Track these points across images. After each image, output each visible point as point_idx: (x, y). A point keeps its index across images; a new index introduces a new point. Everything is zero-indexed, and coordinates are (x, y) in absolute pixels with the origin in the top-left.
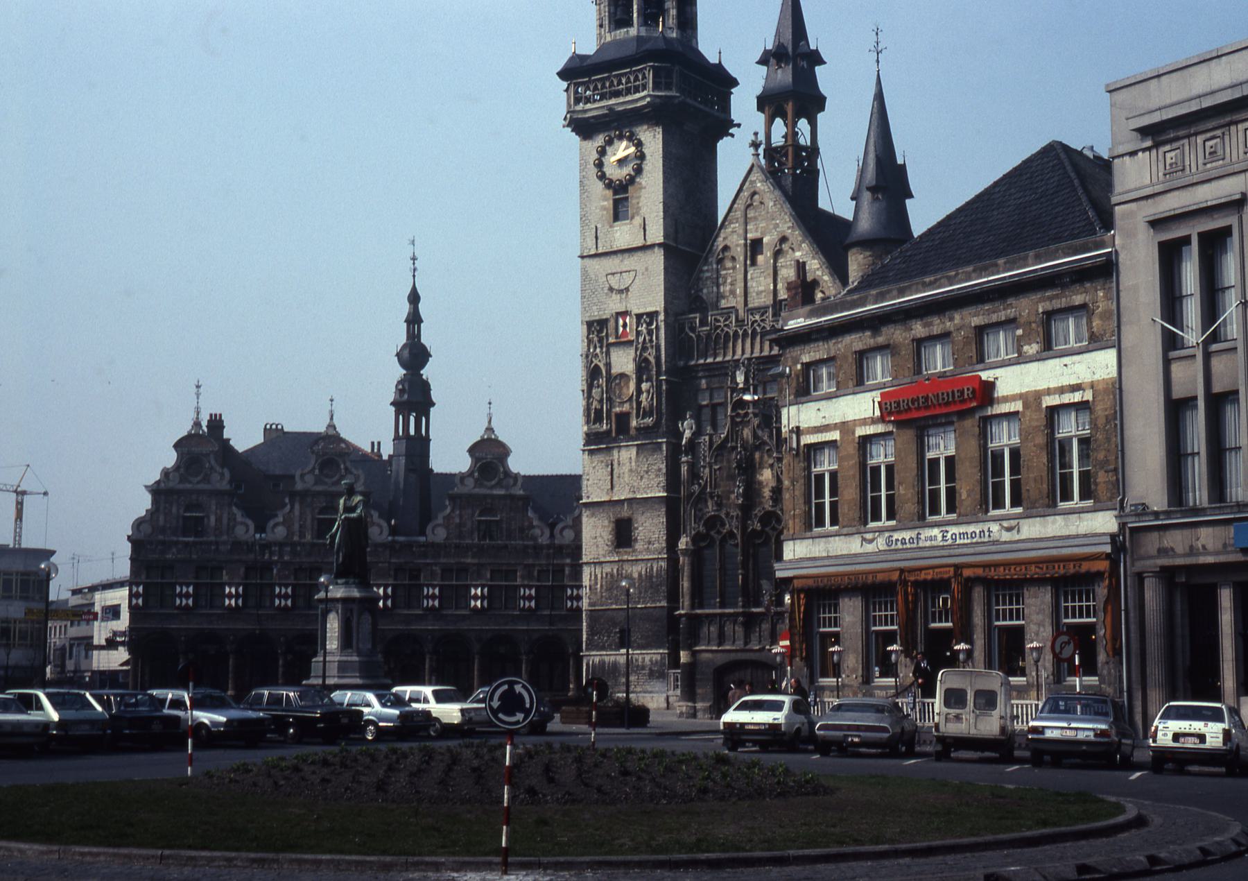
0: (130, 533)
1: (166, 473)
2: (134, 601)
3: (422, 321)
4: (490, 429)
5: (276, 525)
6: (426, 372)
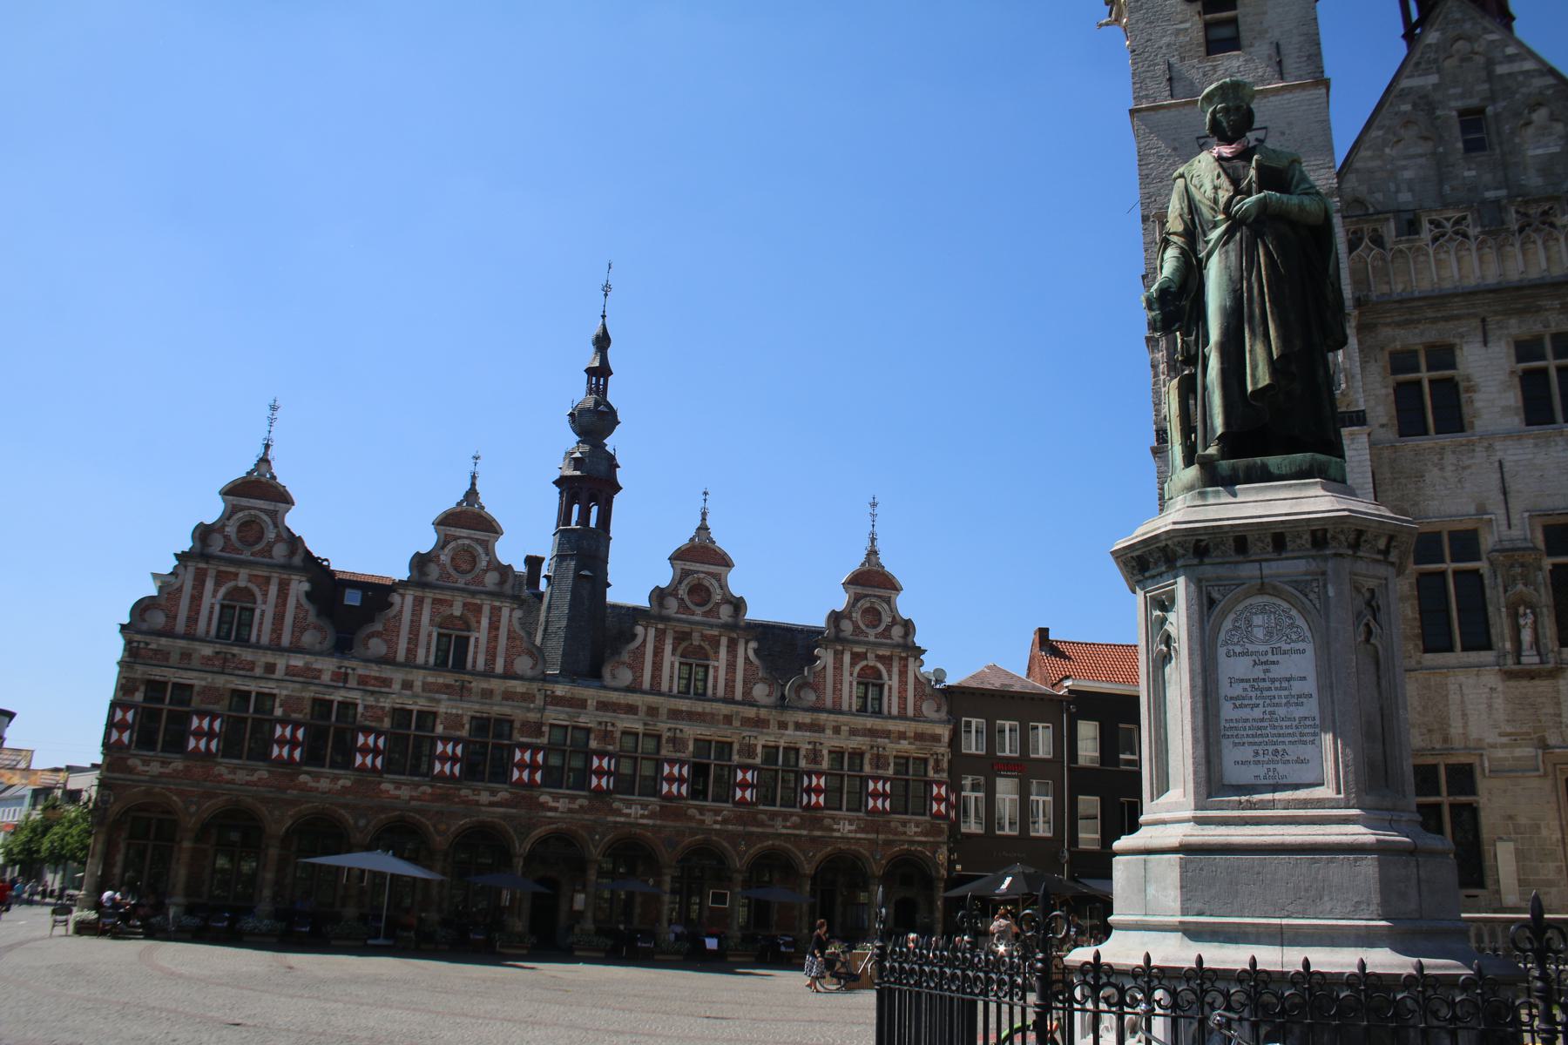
0: (126, 620)
1: (203, 533)
2: (115, 735)
4: (703, 528)
5: (372, 635)
6: (611, 443)
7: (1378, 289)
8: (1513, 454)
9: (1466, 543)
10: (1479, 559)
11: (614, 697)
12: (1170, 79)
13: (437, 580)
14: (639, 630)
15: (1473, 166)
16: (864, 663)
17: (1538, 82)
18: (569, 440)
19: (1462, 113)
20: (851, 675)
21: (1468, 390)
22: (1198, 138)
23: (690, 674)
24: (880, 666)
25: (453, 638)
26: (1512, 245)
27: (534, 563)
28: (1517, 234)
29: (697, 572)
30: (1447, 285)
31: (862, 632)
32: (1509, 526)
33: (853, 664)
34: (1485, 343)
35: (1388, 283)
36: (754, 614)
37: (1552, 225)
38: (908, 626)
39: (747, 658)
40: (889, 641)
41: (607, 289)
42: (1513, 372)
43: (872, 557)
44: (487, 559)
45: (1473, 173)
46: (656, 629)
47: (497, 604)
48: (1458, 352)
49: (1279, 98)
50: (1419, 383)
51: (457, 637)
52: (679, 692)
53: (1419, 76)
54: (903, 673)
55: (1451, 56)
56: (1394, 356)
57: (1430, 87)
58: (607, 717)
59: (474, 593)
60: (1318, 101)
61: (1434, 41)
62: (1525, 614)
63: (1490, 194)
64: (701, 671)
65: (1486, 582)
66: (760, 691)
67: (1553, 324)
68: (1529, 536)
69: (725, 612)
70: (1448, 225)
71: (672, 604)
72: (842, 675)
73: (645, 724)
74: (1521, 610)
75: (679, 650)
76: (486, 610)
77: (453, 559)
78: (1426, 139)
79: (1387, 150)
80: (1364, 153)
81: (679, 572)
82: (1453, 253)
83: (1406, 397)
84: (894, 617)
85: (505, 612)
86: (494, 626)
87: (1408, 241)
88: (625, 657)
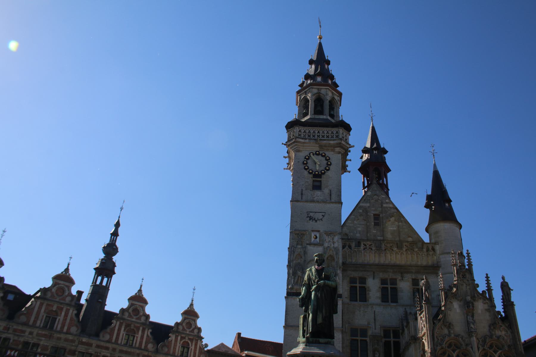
3: (118, 236)
4: (140, 291)
6: (115, 258)
7: (349, 260)
8: (378, 309)
9: (364, 332)
10: (366, 337)
11: (102, 344)
12: (302, 194)
13: (50, 297)
14: (114, 321)
15: (375, 230)
16: (184, 340)
17: (393, 210)
18: (102, 256)
19: (374, 215)
20: (180, 343)
21: (369, 291)
22: (307, 212)
23: (128, 338)
24: (189, 342)
25: (51, 318)
26: (383, 254)
27: (80, 293)
28: (384, 251)
29: (136, 305)
30: (366, 262)
31: (185, 330)
32: (375, 329)
33: (181, 340)
34: (374, 279)
35: (352, 259)
36: (152, 319)
37: (393, 250)
38: (200, 330)
39: (147, 335)
40: (193, 334)
41: (122, 209)
42: (380, 287)
43: (192, 306)
44: (68, 292)
45: (375, 232)
46: (120, 322)
47: (69, 308)
48: (367, 280)
49: (329, 205)
50: (356, 287)
51: (52, 318)
52: (124, 344)
53: (365, 203)
54: (196, 345)
55: (373, 199)
56: (351, 278)
57: (367, 207)
58: (99, 350)
59: (61, 303)
60: (339, 208)
61: (369, 194)
62: (377, 354)
63: (379, 238)
64: (133, 337)
65: (368, 344)
66: (150, 346)
67: (390, 276)
68: (380, 332)
69: (143, 319)
70: (368, 246)
71: (127, 314)
72: (177, 343)
73: (111, 354)
74: (376, 353)
75: (127, 329)
76: (64, 310)
77: (56, 291)
78: (365, 220)
79: (355, 222)
80: (349, 221)
81: (130, 304)
82: (368, 253)
83: (353, 290)
84: (195, 326)
85: (71, 311)
86: (66, 315)
87: (357, 248)
88: (108, 330)
